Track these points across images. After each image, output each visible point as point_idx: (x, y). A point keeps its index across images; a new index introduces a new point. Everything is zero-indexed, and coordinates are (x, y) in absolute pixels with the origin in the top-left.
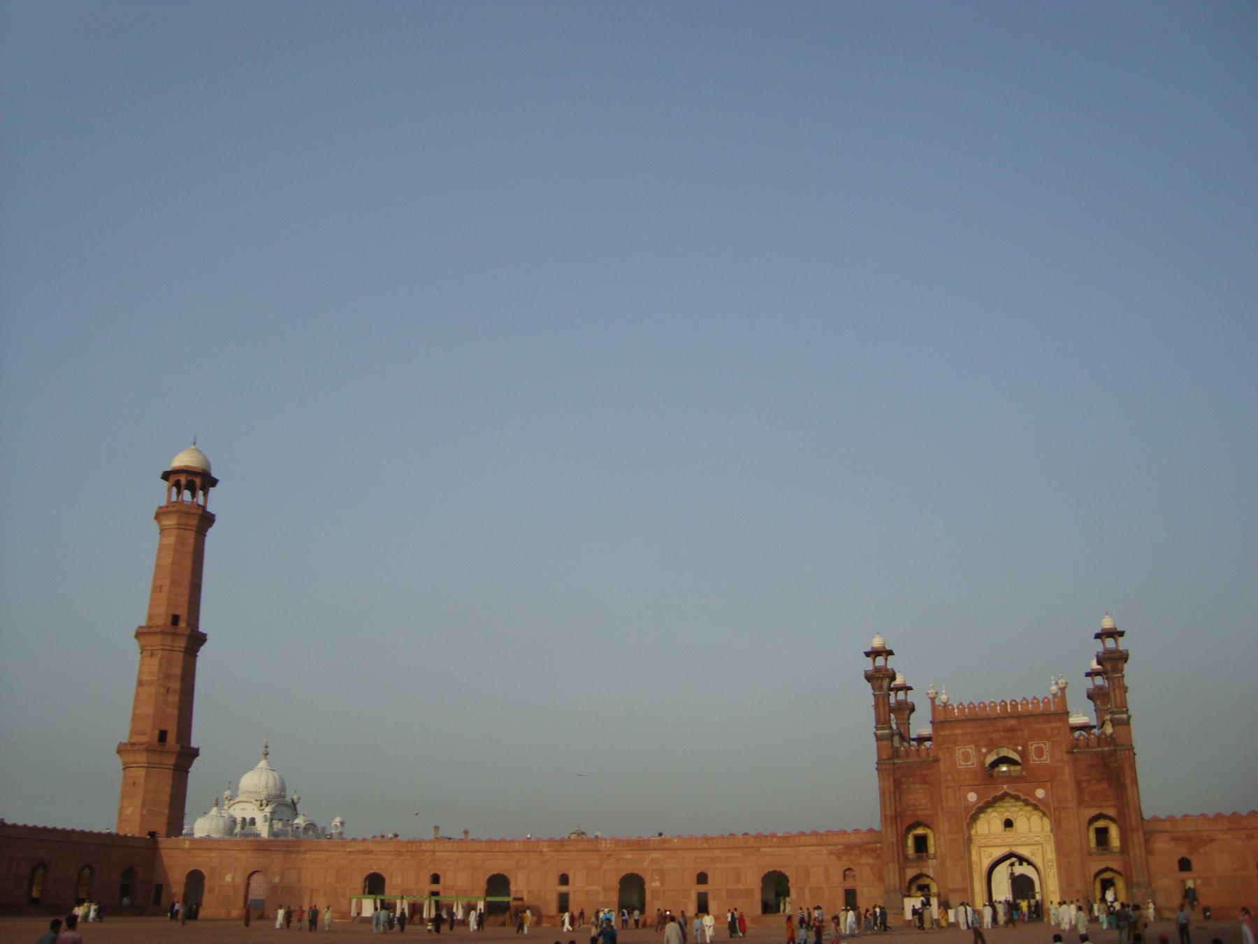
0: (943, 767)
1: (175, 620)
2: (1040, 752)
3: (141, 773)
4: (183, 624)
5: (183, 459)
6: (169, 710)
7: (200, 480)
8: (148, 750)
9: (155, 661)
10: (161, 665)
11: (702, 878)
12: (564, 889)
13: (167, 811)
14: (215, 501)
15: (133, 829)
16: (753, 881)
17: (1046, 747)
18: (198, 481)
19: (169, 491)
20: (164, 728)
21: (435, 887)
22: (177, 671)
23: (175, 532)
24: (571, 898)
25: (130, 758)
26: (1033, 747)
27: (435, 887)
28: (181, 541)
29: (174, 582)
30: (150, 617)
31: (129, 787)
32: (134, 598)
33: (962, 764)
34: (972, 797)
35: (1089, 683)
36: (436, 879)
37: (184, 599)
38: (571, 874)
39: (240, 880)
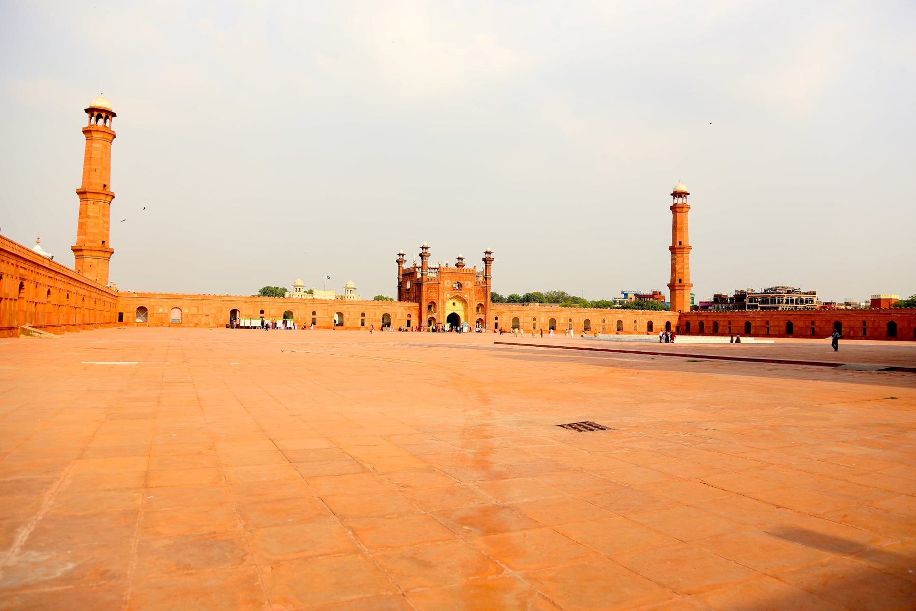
0: (441, 285)
11: (363, 315)
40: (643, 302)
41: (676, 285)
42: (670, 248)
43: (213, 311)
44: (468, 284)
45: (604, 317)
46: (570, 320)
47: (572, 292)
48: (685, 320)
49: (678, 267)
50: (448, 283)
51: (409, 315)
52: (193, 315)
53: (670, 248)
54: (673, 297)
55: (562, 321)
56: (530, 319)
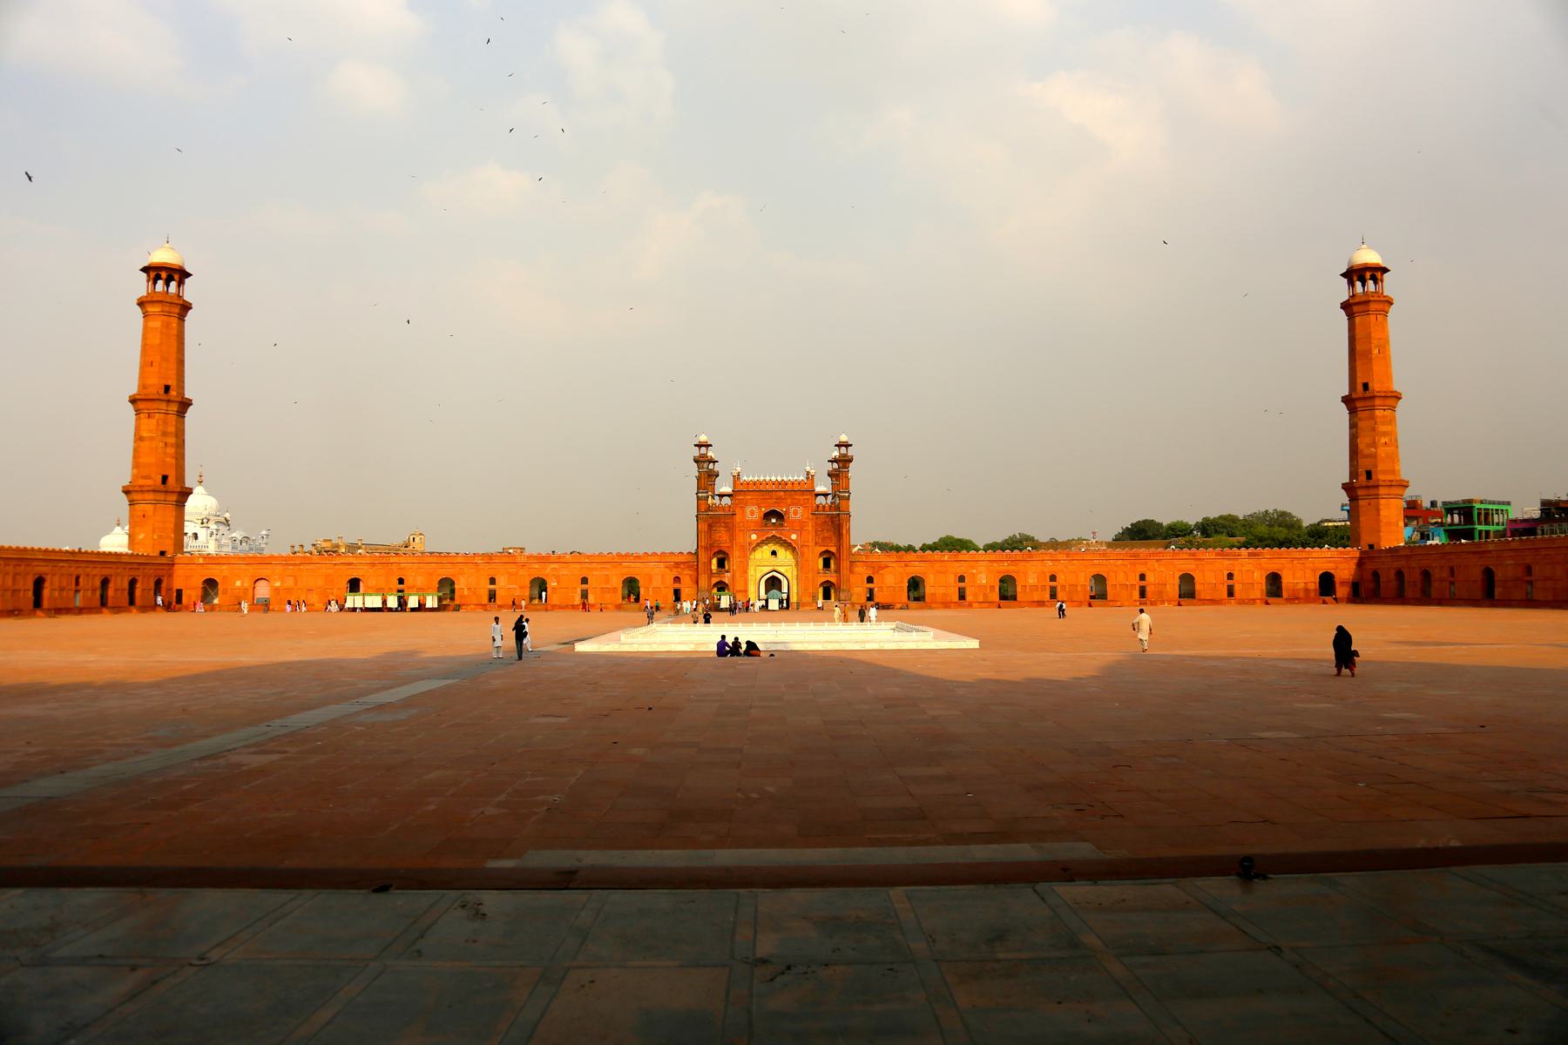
0: (738, 518)
2: (795, 513)
4: (173, 393)
5: (163, 256)
14: (190, 291)
15: (148, 550)
16: (617, 582)
17: (800, 510)
18: (176, 277)
22: (172, 429)
26: (792, 509)
28: (167, 326)
30: (143, 386)
33: (749, 517)
34: (754, 537)
35: (829, 467)
36: (401, 581)
37: (173, 373)
40: (1276, 532)
41: (1362, 485)
42: (1345, 400)
43: (320, 582)
44: (796, 513)
45: (1141, 569)
46: (1053, 578)
47: (1165, 517)
48: (1370, 566)
49: (1362, 443)
50: (753, 513)
51: (677, 579)
52: (288, 590)
53: (1345, 400)
54: (1353, 512)
55: (1032, 581)
56: (952, 579)
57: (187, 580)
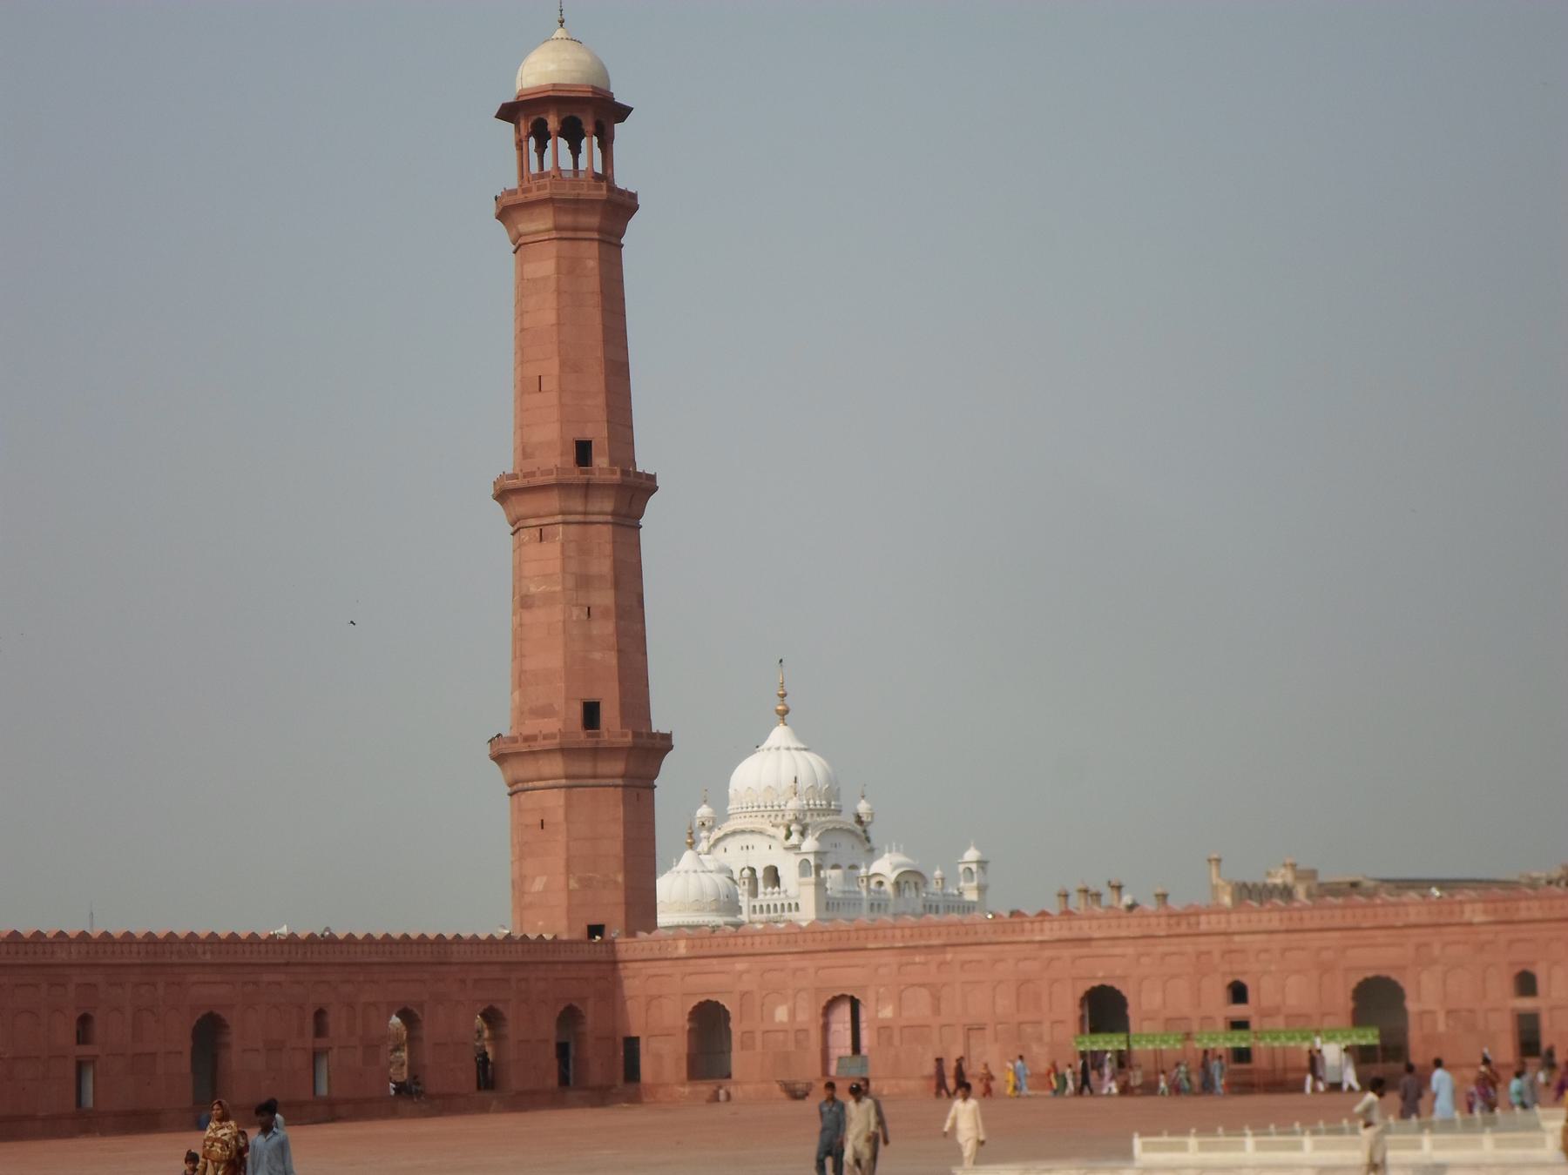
1: (583, 452)
3: (554, 801)
4: (600, 461)
6: (597, 656)
7: (585, 114)
8: (566, 751)
9: (552, 551)
10: (565, 557)
12: (1527, 1004)
13: (620, 878)
14: (634, 157)
19: (520, 145)
20: (592, 696)
21: (1238, 1011)
22: (602, 566)
23: (552, 248)
24: (1545, 1023)
25: (526, 769)
27: (1238, 1011)
28: (569, 269)
29: (570, 366)
30: (525, 452)
31: (530, 838)
32: (476, 404)
36: (1238, 993)
37: (596, 404)
38: (1541, 972)
39: (808, 1015)
57: (657, 1013)
